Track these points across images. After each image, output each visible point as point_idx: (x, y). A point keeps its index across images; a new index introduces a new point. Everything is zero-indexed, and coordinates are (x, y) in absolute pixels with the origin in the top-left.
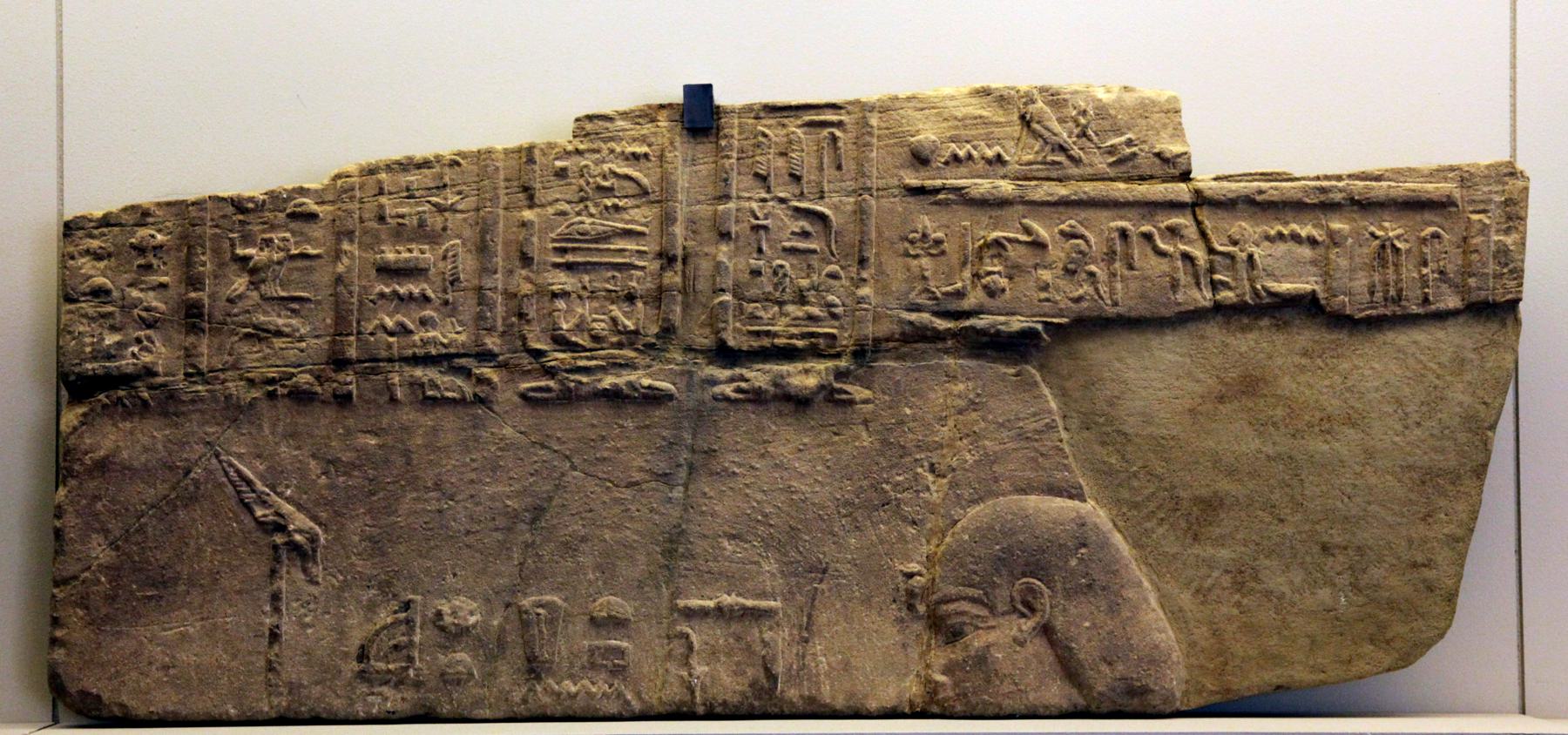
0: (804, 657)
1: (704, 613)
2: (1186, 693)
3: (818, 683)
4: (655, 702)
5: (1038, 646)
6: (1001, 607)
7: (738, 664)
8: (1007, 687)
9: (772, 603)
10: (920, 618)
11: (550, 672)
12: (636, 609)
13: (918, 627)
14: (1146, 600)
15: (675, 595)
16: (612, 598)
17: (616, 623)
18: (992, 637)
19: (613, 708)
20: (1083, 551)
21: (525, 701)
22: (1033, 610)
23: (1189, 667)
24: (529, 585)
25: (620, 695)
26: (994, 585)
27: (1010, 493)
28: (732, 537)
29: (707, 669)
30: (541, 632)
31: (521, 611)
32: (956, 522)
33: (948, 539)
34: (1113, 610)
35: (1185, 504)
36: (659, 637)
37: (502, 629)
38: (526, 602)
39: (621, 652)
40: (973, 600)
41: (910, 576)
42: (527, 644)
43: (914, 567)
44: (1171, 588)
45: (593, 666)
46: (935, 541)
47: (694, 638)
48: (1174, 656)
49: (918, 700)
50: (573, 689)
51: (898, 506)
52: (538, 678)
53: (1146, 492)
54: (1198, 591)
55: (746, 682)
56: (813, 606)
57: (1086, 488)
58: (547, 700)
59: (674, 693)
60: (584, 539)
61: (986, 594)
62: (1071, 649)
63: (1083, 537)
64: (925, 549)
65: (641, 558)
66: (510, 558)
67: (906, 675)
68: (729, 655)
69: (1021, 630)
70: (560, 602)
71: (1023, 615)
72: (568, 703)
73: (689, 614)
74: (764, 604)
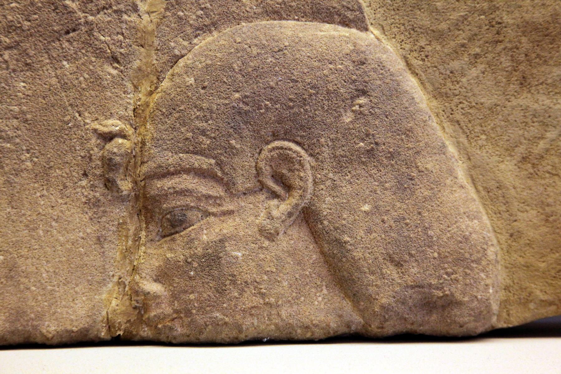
2: (504, 304)
5: (296, 239)
6: (242, 183)
8: (250, 300)
10: (122, 199)
13: (120, 212)
14: (451, 172)
18: (228, 227)
20: (362, 100)
22: (289, 188)
23: (511, 268)
26: (231, 151)
27: (257, 16)
32: (176, 59)
33: (165, 84)
34: (404, 186)
35: (510, 33)
40: (201, 173)
41: (108, 137)
43: (113, 124)
44: (486, 154)
46: (146, 87)
48: (491, 252)
49: (120, 319)
51: (90, 33)
53: (454, 16)
54: (524, 159)
57: (367, 11)
61: (220, 164)
62: (341, 244)
63: (362, 81)
64: (131, 99)
67: (103, 283)
69: (270, 217)
71: (275, 195)
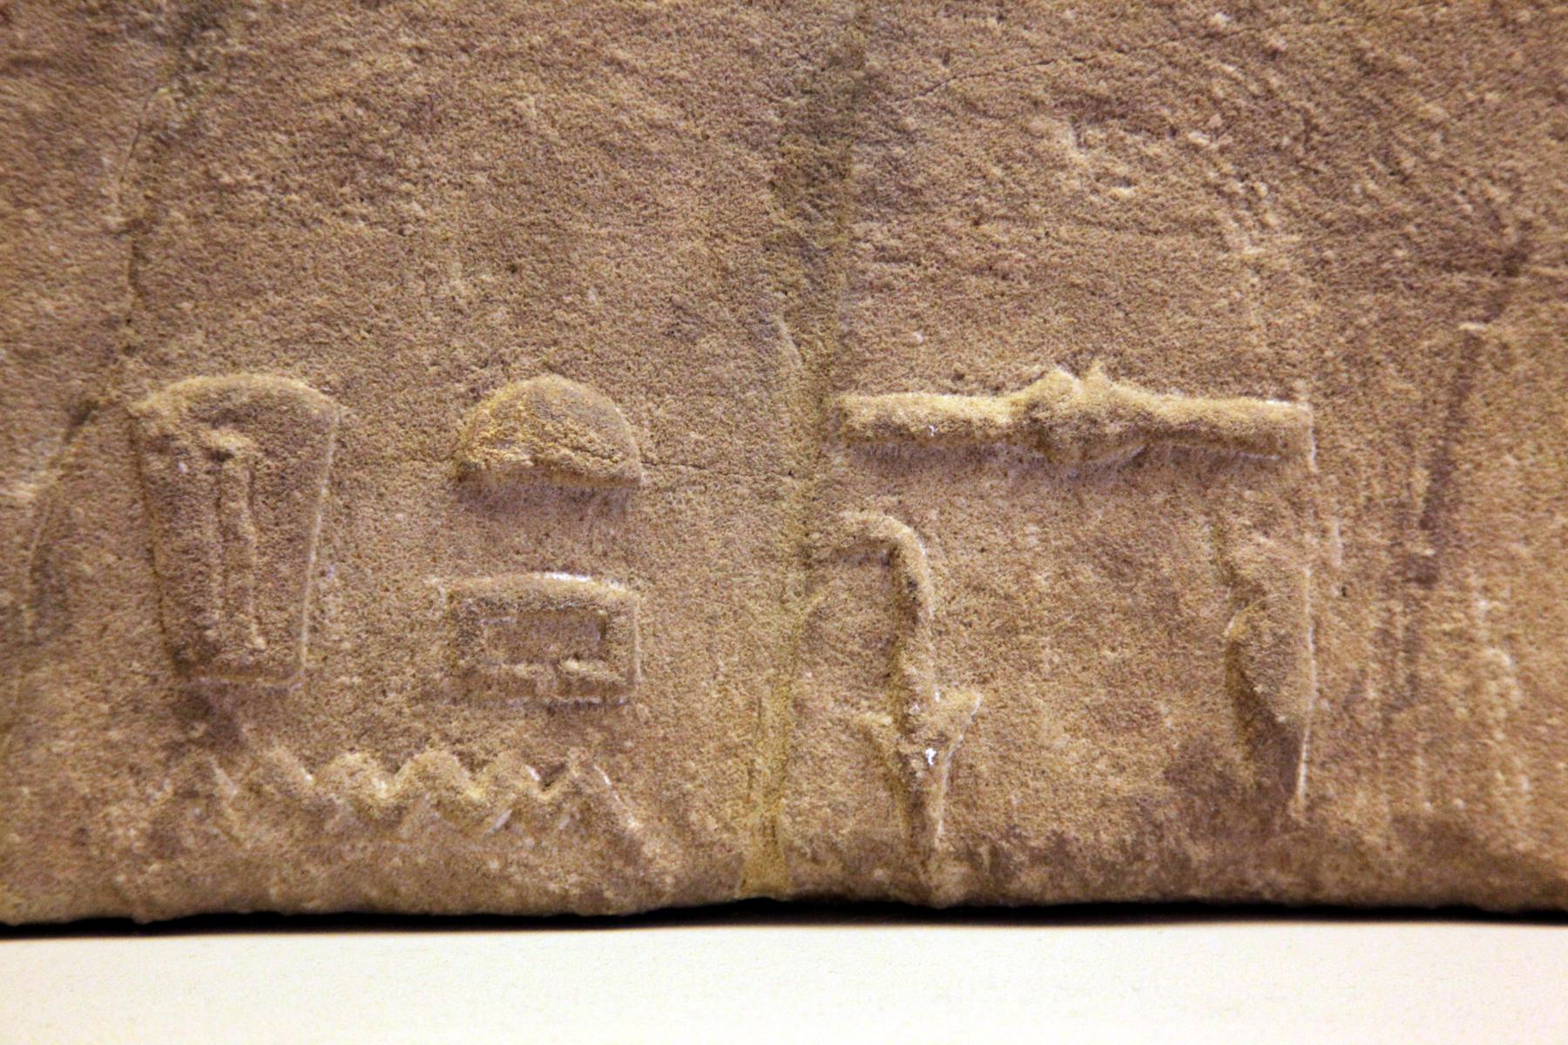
0: (1412, 647)
1: (967, 450)
3: (1478, 763)
4: (748, 845)
7: (1116, 679)
9: (1275, 409)
11: (275, 711)
12: (662, 434)
15: (836, 370)
16: (547, 380)
17: (575, 497)
19: (563, 873)
21: (162, 842)
24: (174, 324)
25: (591, 816)
28: (1090, 109)
29: (977, 698)
30: (229, 533)
31: (144, 443)
36: (765, 555)
37: (55, 524)
38: (162, 402)
39: (596, 628)
42: (172, 588)
45: (469, 685)
47: (920, 561)
50: (383, 790)
52: (224, 740)
55: (1154, 755)
56: (1457, 419)
58: (261, 836)
59: (831, 811)
60: (422, 117)
65: (684, 203)
66: (83, 199)
68: (1078, 634)
70: (317, 402)
72: (359, 850)
73: (899, 454)
74: (1235, 410)
